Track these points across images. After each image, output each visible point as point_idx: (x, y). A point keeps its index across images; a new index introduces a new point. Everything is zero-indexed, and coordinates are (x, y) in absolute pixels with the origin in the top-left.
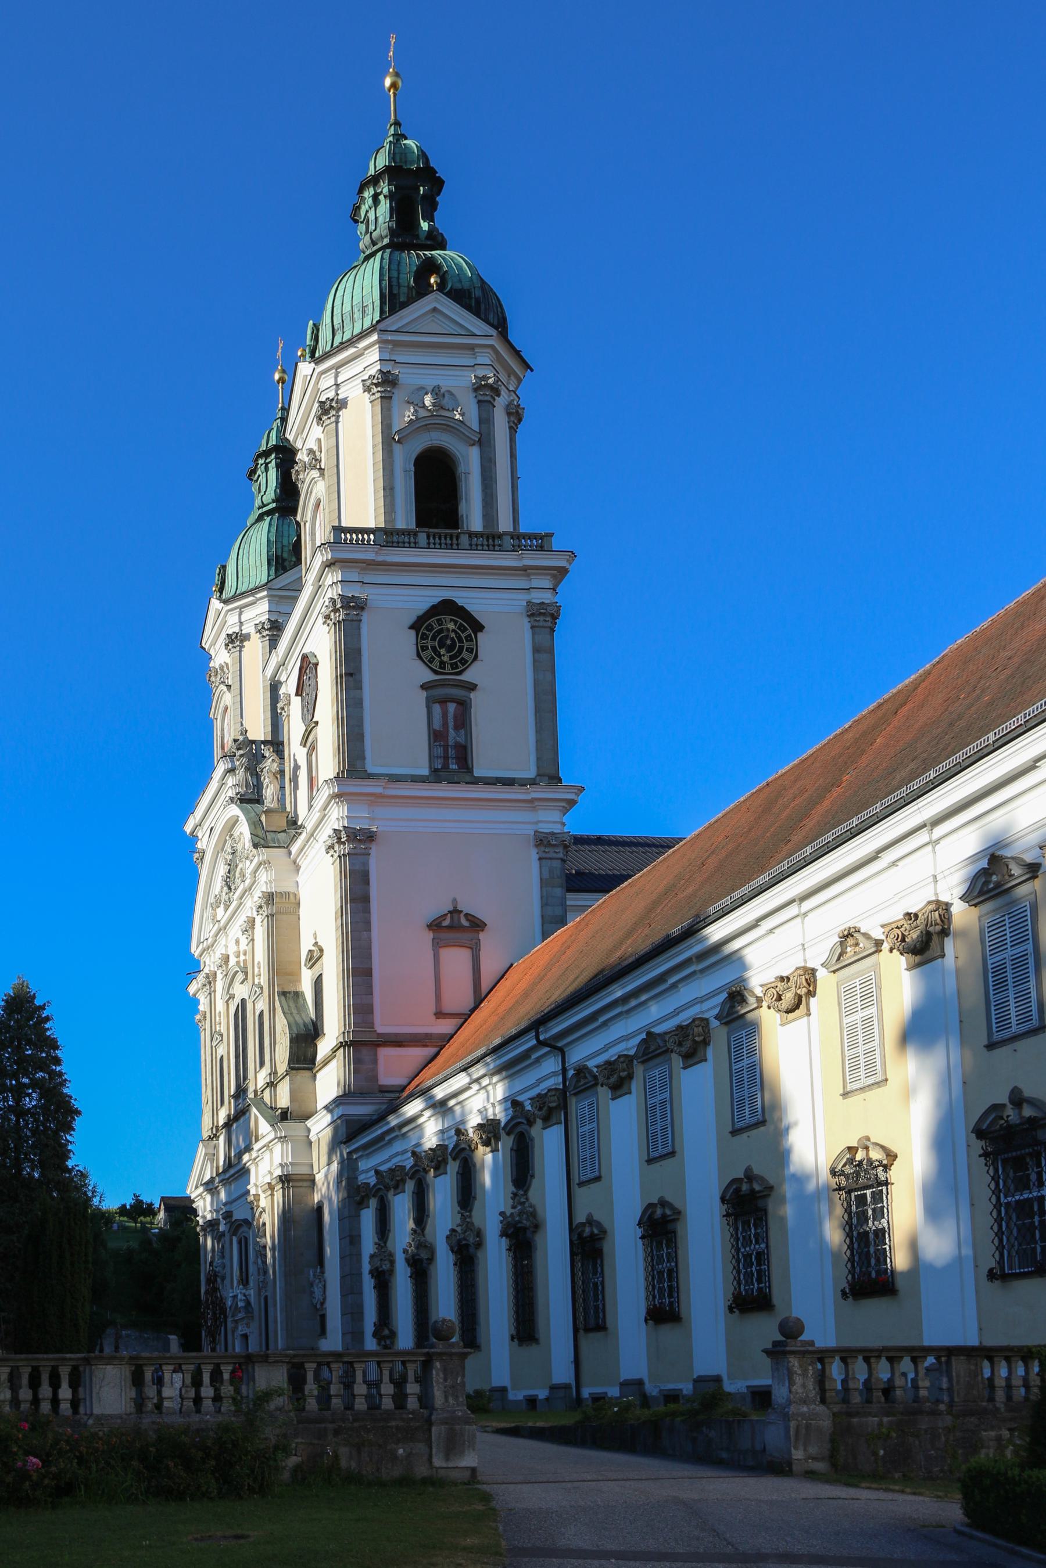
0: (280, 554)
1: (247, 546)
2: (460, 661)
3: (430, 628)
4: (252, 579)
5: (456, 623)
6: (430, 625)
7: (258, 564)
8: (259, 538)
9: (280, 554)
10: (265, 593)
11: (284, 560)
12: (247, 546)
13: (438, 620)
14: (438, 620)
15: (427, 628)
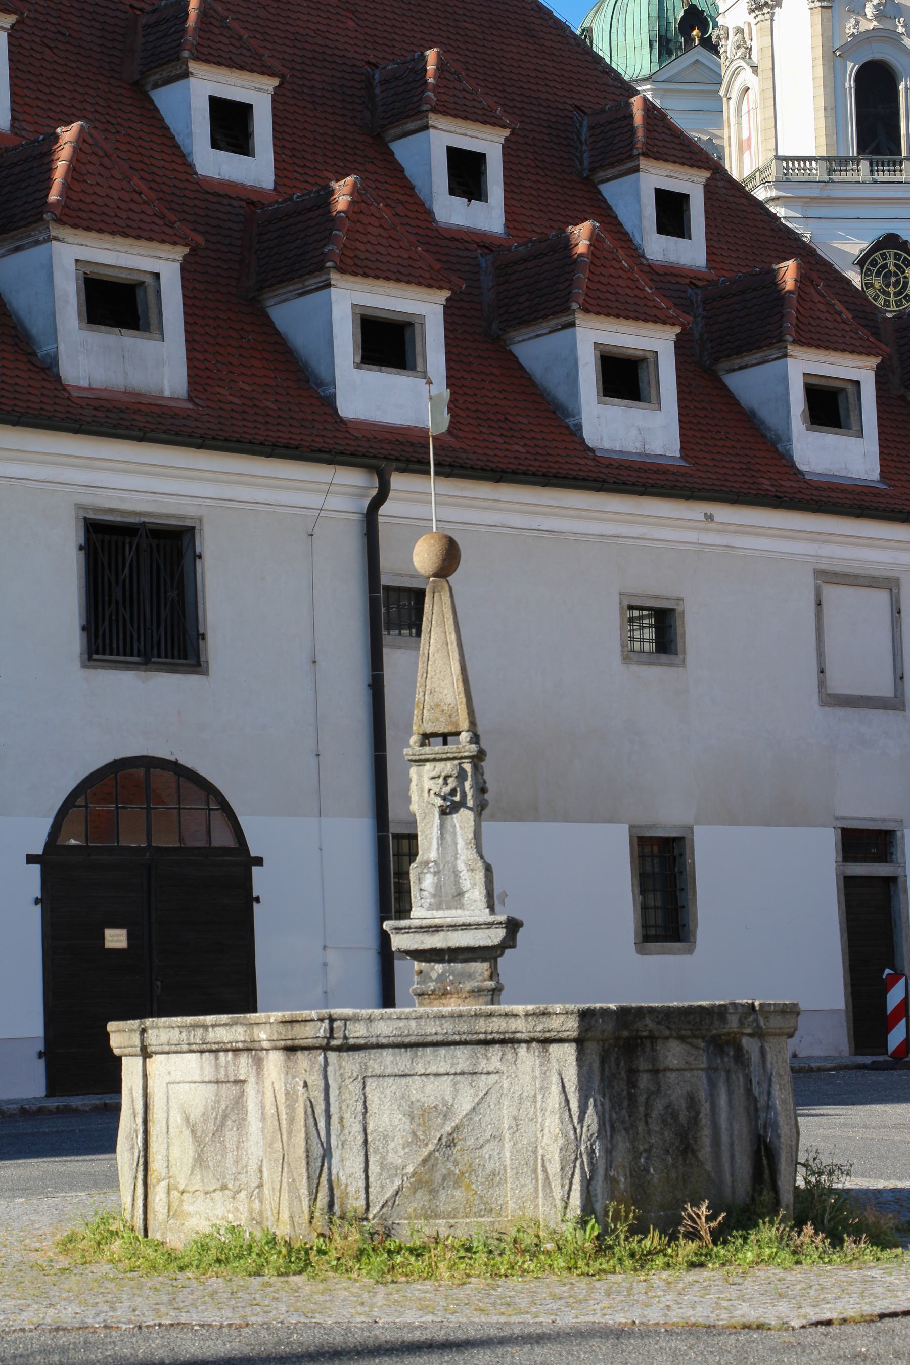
0: (663, 33)
1: (622, 16)
2: (904, 298)
3: (874, 263)
4: (631, 62)
5: (897, 257)
6: (874, 260)
7: (638, 43)
8: (637, 9)
9: (663, 33)
10: (649, 87)
11: (669, 41)
12: (622, 16)
13: (882, 255)
14: (882, 255)
15: (871, 264)
